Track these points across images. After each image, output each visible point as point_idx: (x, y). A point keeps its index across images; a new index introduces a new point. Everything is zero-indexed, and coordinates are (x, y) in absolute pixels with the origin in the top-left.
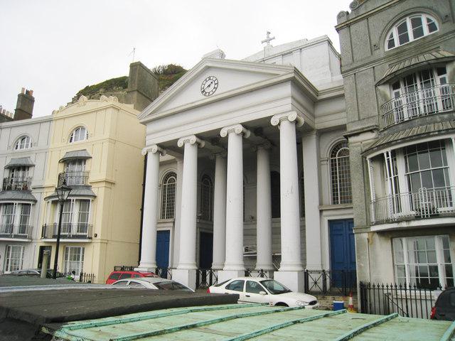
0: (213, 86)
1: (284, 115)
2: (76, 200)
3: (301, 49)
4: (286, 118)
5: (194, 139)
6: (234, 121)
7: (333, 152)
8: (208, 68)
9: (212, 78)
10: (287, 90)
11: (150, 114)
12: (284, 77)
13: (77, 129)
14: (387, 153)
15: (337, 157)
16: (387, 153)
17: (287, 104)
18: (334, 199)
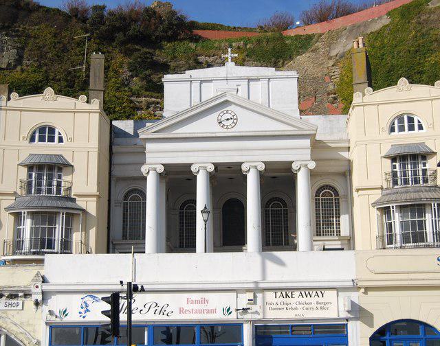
0: (231, 121)
1: (303, 163)
2: (28, 212)
3: (269, 79)
4: (306, 166)
5: (211, 168)
6: (255, 158)
7: (317, 192)
8: (227, 103)
9: (229, 112)
10: (307, 143)
11: (154, 132)
12: (308, 132)
13: (42, 130)
14: (393, 207)
15: (321, 198)
16: (393, 207)
17: (307, 154)
18: (317, 232)
